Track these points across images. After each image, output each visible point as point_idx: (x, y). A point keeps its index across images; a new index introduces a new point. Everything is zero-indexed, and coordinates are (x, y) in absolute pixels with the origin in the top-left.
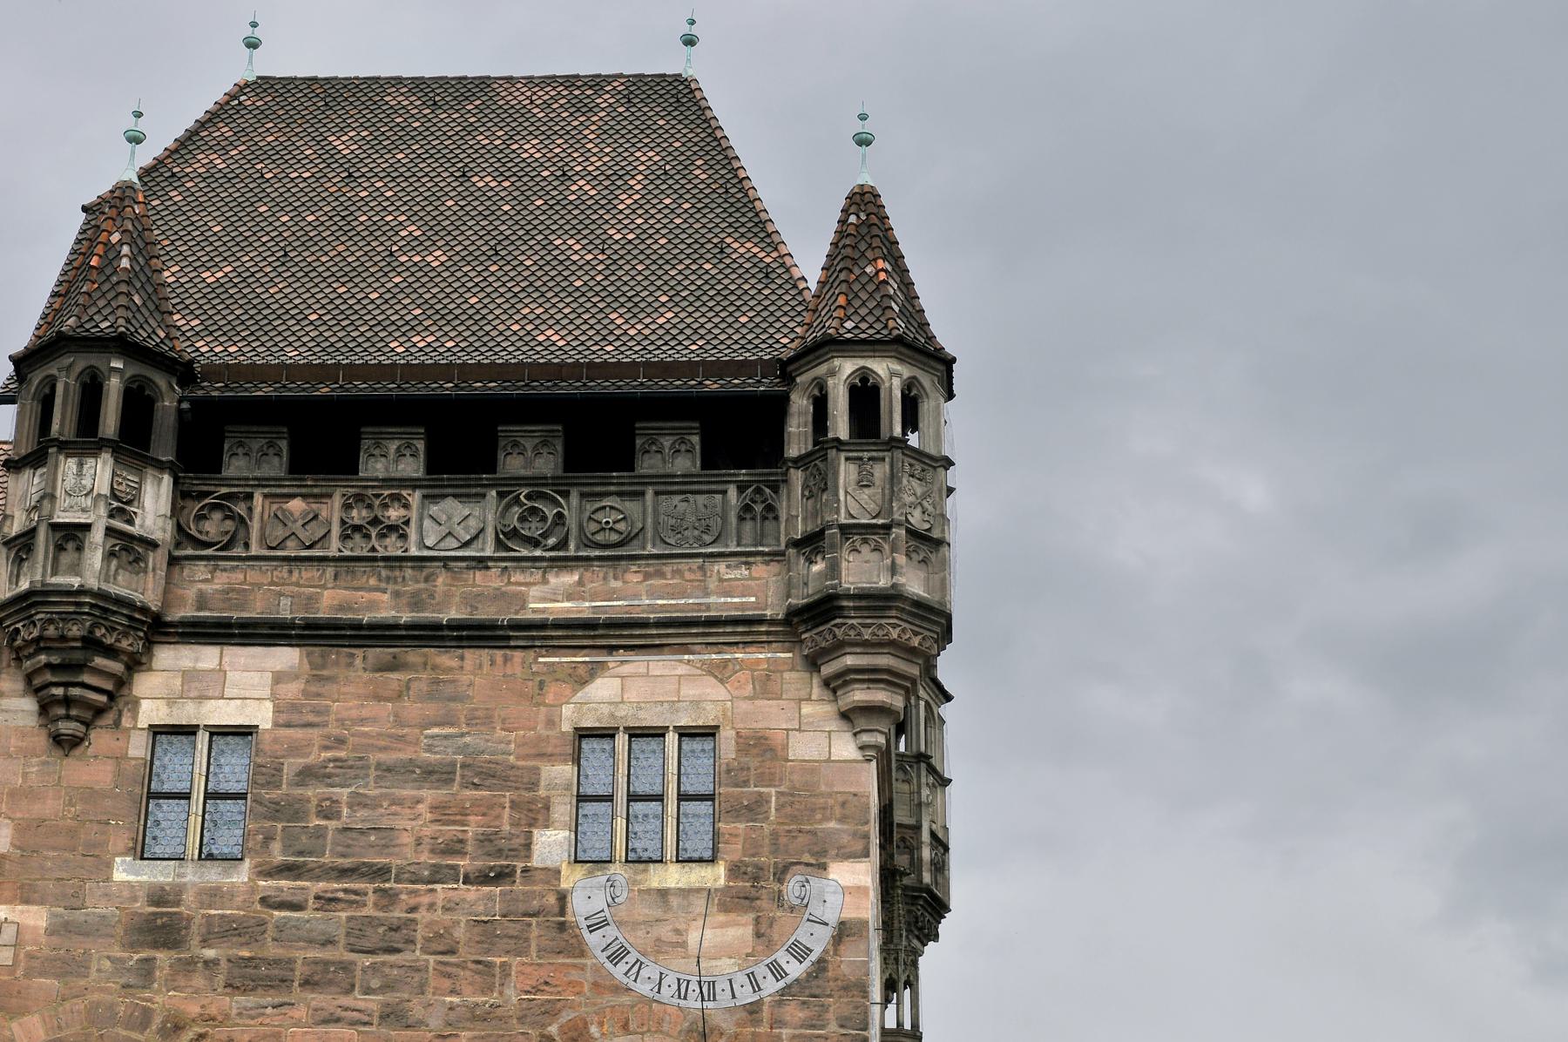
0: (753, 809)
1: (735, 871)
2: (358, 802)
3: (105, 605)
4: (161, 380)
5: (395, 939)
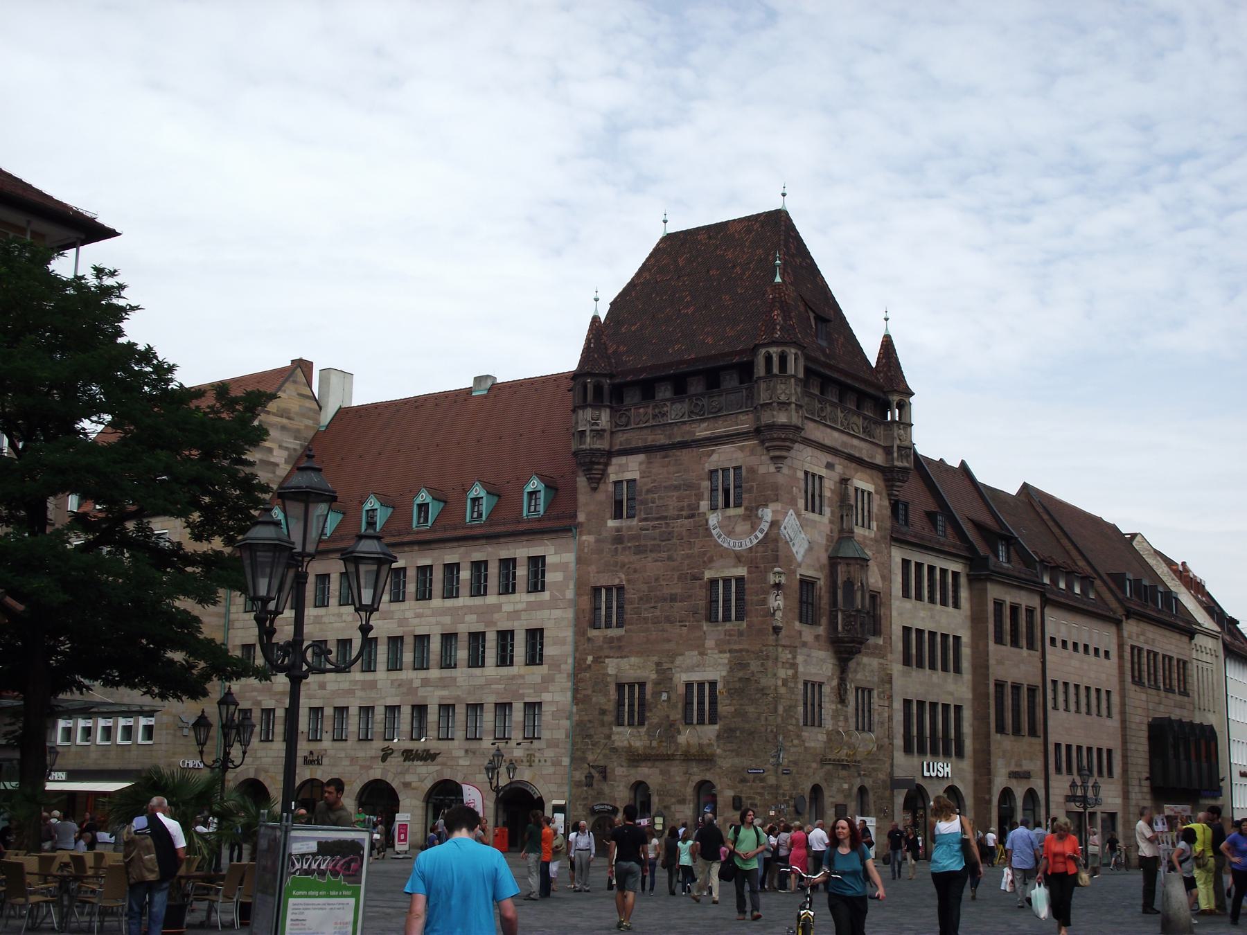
0: (750, 490)
1: (746, 509)
2: (660, 498)
3: (593, 452)
4: (603, 380)
5: (668, 537)
